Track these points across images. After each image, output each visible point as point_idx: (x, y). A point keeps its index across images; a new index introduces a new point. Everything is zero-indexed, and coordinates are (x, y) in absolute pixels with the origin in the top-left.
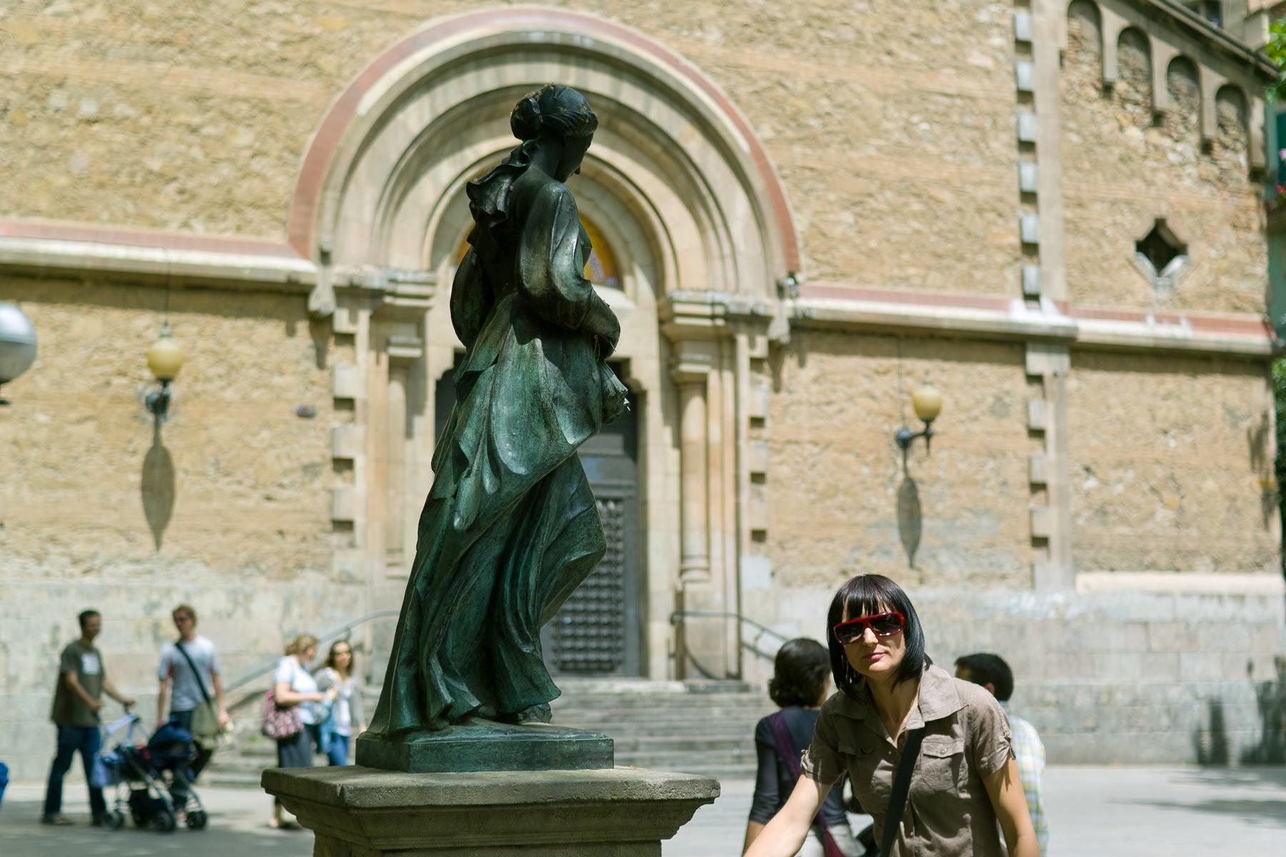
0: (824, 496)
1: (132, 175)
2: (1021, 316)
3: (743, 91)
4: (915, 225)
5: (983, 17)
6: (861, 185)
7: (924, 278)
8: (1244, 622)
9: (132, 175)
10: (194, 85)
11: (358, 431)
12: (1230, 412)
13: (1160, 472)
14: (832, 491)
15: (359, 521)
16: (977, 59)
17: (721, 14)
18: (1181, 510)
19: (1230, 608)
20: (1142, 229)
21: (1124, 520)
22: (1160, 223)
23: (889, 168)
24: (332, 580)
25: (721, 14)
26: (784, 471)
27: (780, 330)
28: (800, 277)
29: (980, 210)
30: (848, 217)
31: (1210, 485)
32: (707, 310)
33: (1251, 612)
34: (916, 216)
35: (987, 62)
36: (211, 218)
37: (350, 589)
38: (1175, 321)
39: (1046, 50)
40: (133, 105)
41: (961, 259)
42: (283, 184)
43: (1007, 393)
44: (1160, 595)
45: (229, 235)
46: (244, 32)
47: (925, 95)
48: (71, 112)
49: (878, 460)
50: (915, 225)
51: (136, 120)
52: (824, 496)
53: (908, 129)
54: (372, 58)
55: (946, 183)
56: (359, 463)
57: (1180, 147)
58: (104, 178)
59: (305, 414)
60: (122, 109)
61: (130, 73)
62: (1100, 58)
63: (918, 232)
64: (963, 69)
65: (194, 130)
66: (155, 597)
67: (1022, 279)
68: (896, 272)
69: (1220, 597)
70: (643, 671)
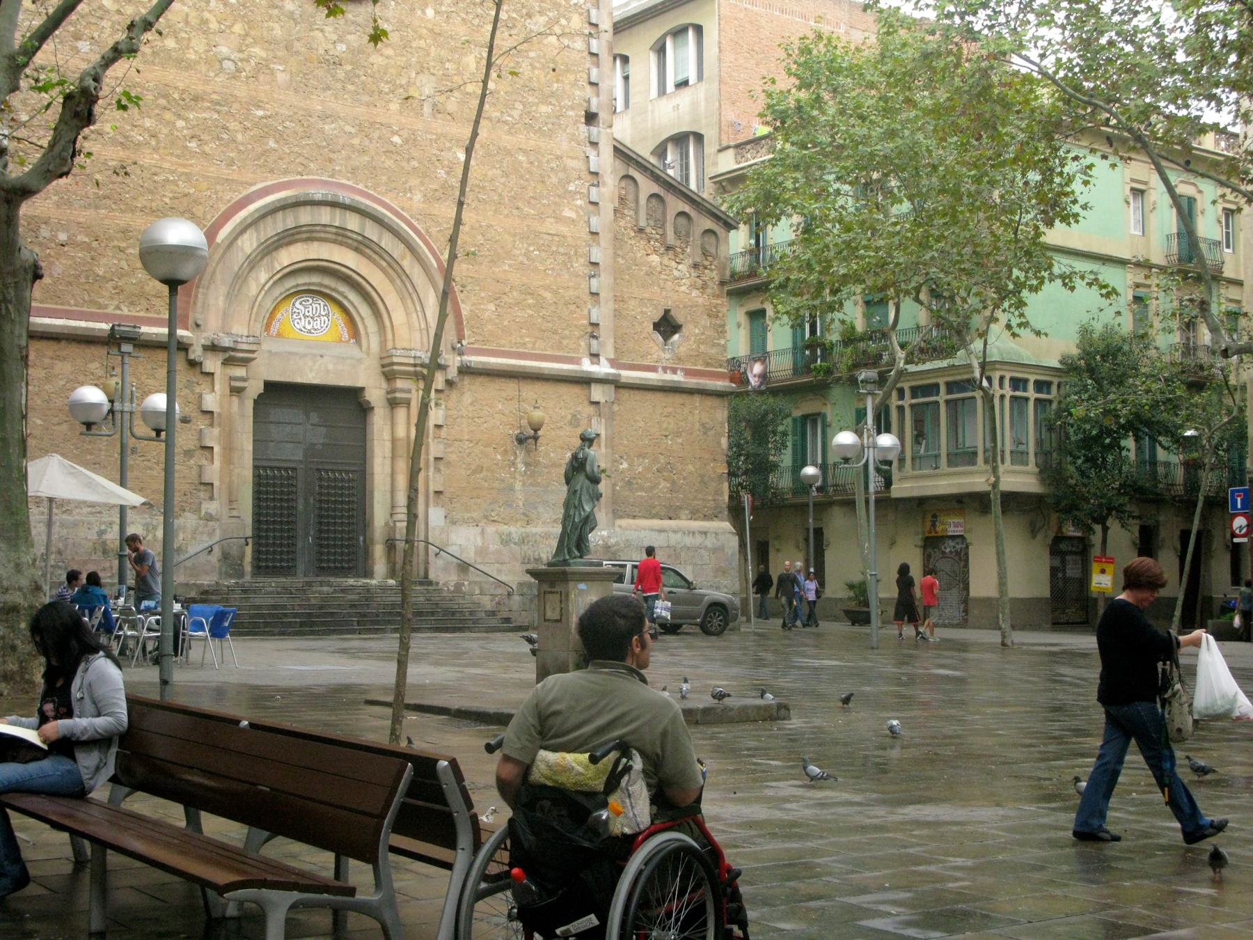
0: (475, 472)
1: (87, 278)
2: (587, 366)
3: (434, 230)
4: (530, 312)
5: (572, 188)
7: (534, 344)
8: (706, 548)
9: (87, 278)
10: (122, 223)
11: (216, 431)
12: (703, 425)
13: (662, 460)
14: (480, 469)
15: (216, 484)
16: (568, 213)
17: (422, 183)
18: (673, 483)
19: (699, 540)
20: (657, 316)
21: (642, 488)
22: (667, 312)
24: (201, 519)
25: (422, 183)
26: (453, 457)
27: (452, 373)
28: (464, 342)
29: (567, 304)
30: (492, 307)
31: (691, 467)
32: (412, 361)
33: (710, 542)
34: (530, 306)
35: (573, 215)
36: (132, 303)
37: (211, 523)
38: (674, 371)
39: (608, 208)
40: (87, 235)
41: (555, 332)
43: (579, 412)
44: (661, 531)
45: (142, 314)
46: (151, 192)
47: (537, 234)
48: (52, 239)
49: (506, 451)
50: (530, 312)
51: (89, 245)
52: (475, 472)
53: (527, 254)
54: (223, 208)
55: (547, 288)
56: (216, 449)
57: (680, 267)
58: (71, 279)
60: (81, 238)
61: (86, 216)
62: (637, 212)
63: (531, 316)
64: (559, 219)
65: (122, 250)
66: (103, 527)
67: (590, 346)
68: (519, 340)
69: (694, 533)
70: (368, 574)
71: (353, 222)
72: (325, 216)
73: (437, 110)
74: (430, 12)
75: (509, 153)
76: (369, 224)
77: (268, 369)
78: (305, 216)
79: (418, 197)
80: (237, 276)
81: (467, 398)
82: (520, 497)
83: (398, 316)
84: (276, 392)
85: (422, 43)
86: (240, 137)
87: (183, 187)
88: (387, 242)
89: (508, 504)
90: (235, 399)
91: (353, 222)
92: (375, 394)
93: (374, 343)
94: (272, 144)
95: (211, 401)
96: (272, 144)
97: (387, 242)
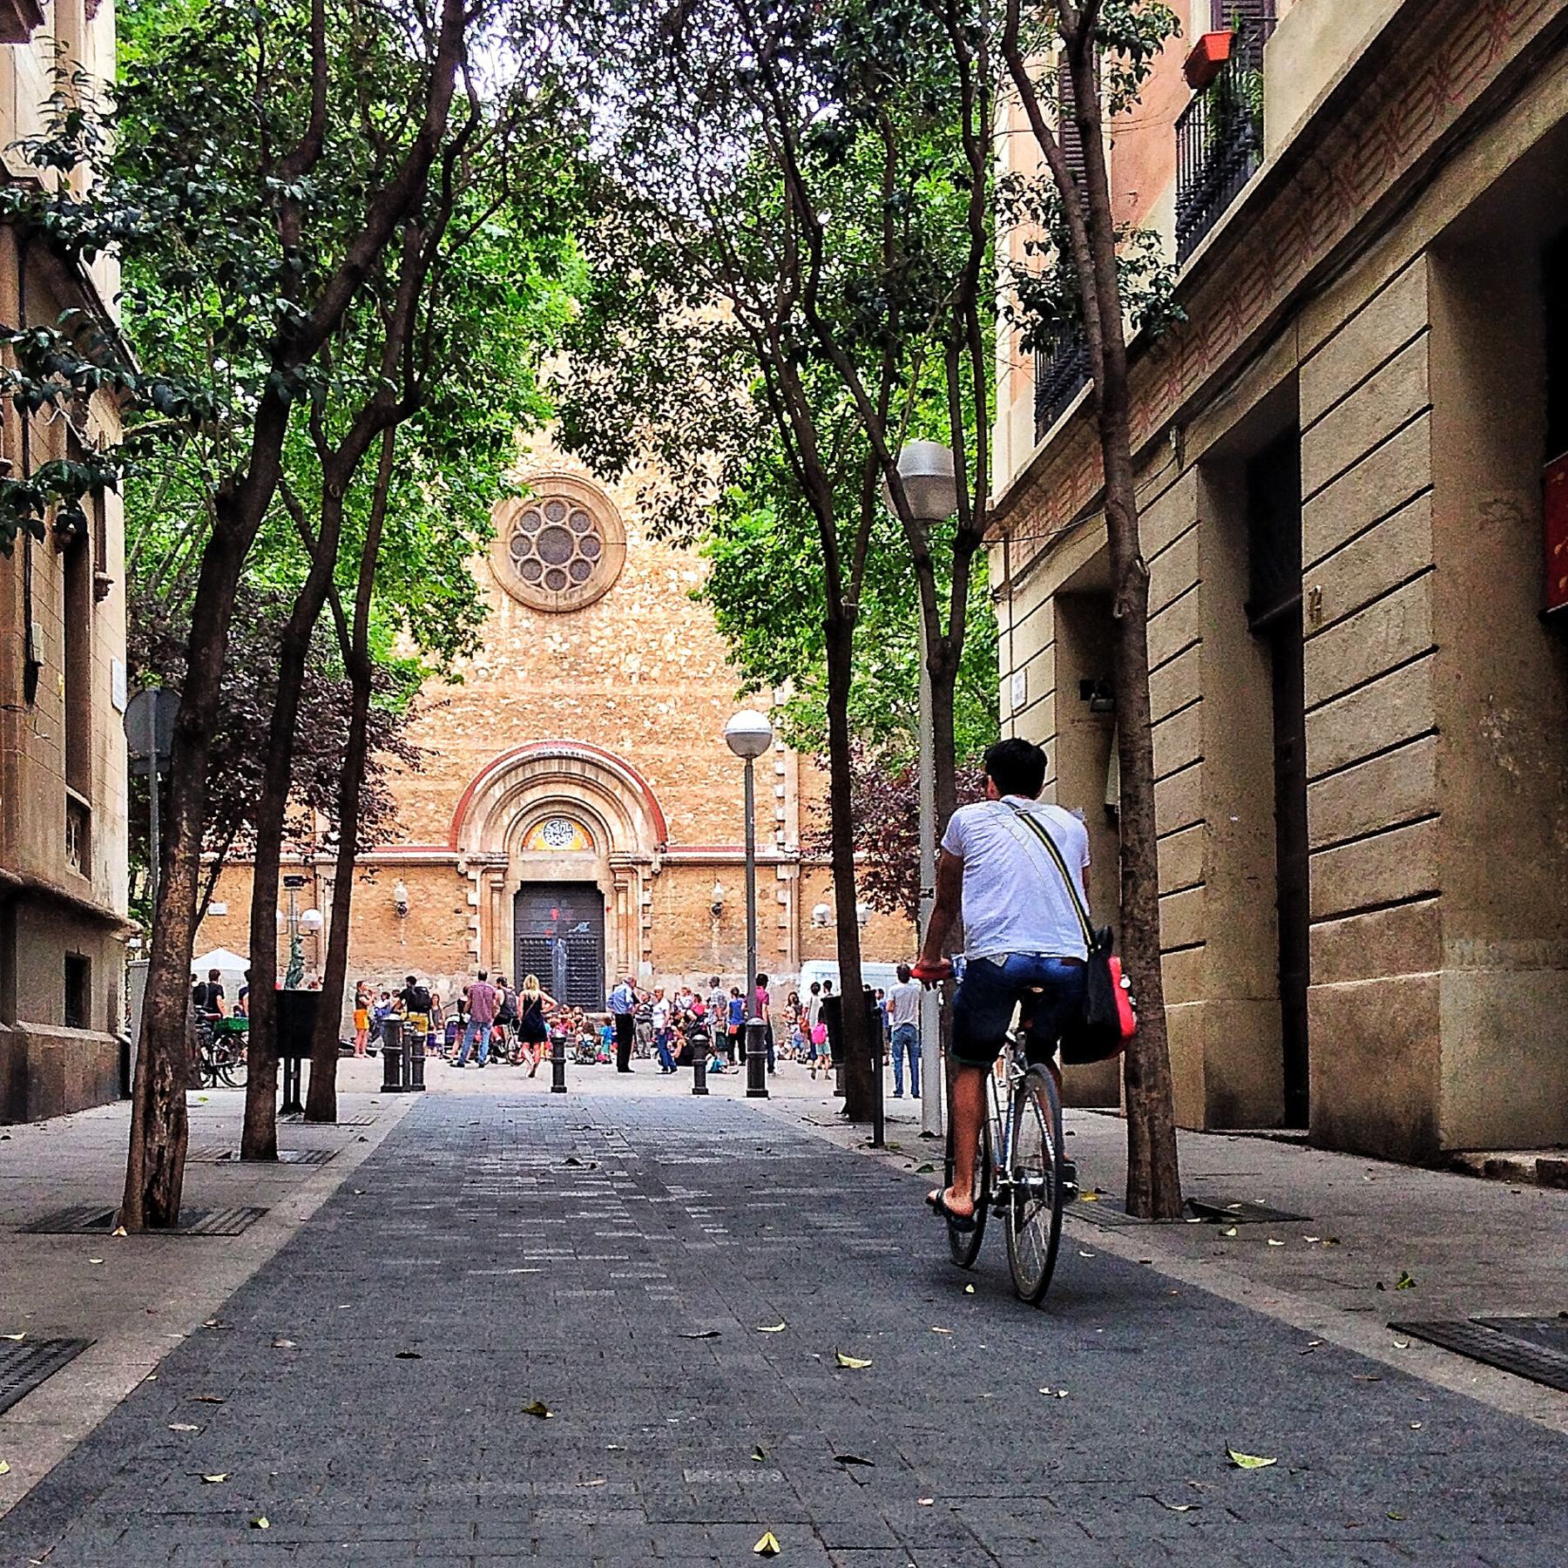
3: (641, 766)
6: (698, 800)
11: (477, 917)
23: (710, 793)
26: (659, 926)
27: (656, 866)
30: (691, 816)
42: (447, 823)
59: (457, 912)
71: (576, 768)
72: (554, 766)
73: (642, 678)
74: (636, 607)
75: (703, 700)
76: (588, 766)
77: (520, 873)
78: (539, 769)
79: (628, 745)
80: (490, 815)
81: (671, 883)
82: (716, 953)
83: (617, 829)
84: (529, 888)
85: (629, 632)
86: (492, 720)
87: (453, 759)
88: (603, 779)
89: (706, 958)
90: (496, 896)
91: (576, 768)
92: (603, 887)
93: (604, 852)
94: (515, 721)
95: (474, 898)
96: (515, 721)
97: (603, 779)
